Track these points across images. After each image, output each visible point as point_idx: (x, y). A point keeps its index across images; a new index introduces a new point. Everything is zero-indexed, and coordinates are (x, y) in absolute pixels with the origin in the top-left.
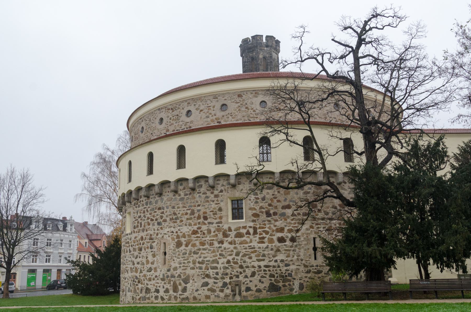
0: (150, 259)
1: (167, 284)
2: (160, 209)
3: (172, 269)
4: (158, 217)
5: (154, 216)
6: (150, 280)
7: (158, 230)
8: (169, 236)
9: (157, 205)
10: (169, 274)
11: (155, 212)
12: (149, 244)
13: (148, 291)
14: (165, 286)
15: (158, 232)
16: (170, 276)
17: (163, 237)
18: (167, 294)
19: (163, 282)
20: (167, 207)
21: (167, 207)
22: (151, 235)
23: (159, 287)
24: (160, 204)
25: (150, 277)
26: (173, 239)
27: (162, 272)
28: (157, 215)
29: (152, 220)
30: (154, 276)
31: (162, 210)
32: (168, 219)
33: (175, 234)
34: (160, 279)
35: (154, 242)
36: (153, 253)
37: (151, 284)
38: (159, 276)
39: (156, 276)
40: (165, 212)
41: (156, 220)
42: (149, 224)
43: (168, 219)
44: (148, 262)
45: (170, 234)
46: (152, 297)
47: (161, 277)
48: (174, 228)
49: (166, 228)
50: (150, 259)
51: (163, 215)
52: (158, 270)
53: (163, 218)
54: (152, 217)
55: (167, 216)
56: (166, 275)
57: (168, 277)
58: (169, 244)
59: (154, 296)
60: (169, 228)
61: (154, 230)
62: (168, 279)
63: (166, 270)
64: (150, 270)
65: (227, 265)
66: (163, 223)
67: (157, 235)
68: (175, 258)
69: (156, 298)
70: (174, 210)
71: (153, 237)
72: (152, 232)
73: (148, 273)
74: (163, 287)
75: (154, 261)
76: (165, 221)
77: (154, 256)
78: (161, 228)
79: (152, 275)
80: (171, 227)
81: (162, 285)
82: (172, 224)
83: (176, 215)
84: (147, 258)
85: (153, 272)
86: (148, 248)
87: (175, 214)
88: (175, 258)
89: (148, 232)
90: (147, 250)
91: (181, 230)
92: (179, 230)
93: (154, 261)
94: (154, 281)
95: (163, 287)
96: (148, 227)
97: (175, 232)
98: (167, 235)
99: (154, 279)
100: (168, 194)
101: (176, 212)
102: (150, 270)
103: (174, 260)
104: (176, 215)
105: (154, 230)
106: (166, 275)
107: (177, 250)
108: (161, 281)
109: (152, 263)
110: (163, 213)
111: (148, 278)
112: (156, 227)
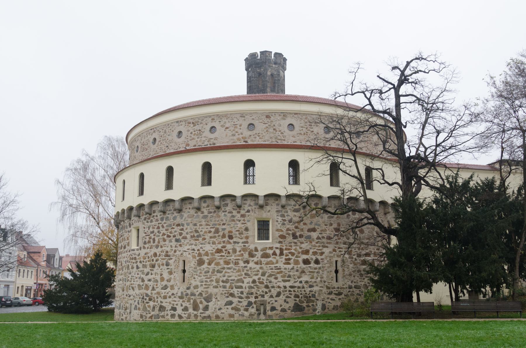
0: (166, 276)
1: (186, 302)
2: (178, 225)
3: (192, 287)
4: (176, 233)
5: (171, 233)
6: (165, 297)
7: (176, 247)
8: (189, 254)
9: (175, 221)
10: (189, 292)
11: (173, 228)
12: (164, 262)
13: (162, 308)
14: (183, 304)
15: (176, 249)
16: (189, 294)
17: (182, 254)
18: (186, 312)
19: (181, 300)
20: (188, 224)
21: (188, 224)
22: (167, 252)
23: (177, 305)
24: (178, 220)
25: (166, 294)
26: (194, 257)
27: (181, 290)
28: (176, 232)
29: (169, 236)
30: (170, 294)
31: (182, 227)
32: (188, 236)
33: (196, 251)
34: (177, 297)
35: (171, 259)
36: (169, 270)
37: (166, 302)
38: (177, 293)
39: (173, 294)
40: (185, 229)
41: (174, 236)
42: (164, 240)
43: (188, 236)
44: (162, 279)
45: (191, 252)
46: (167, 315)
47: (179, 294)
48: (196, 245)
49: (186, 245)
50: (166, 276)
51: (182, 232)
52: (176, 288)
53: (183, 235)
54: (169, 233)
55: (187, 233)
56: (184, 293)
57: (187, 295)
58: (189, 262)
59: (170, 315)
60: (189, 245)
61: (171, 246)
62: (188, 297)
63: (185, 288)
64: (165, 287)
65: (252, 285)
66: (182, 240)
67: (175, 251)
68: (196, 277)
69: (173, 316)
70: (196, 227)
71: (169, 253)
72: (168, 249)
73: (163, 291)
74: (182, 305)
75: (171, 278)
76: (185, 238)
77: (170, 273)
78: (180, 245)
79: (168, 293)
80: (192, 244)
81: (179, 303)
82: (193, 242)
83: (198, 232)
84: (161, 275)
85: (169, 289)
86: (163, 265)
87: (196, 231)
88: (196, 277)
89: (164, 248)
90: (161, 268)
91: (204, 249)
92: (201, 248)
93: (171, 278)
94: (171, 299)
95: (182, 305)
96: (164, 243)
97: (196, 249)
98: (187, 253)
99: (170, 297)
100: (190, 210)
101: (197, 229)
102: (165, 287)
103: (194, 278)
104: (198, 232)
105: (171, 246)
106: (184, 293)
107: (198, 268)
108: (179, 300)
109: (169, 281)
110: (182, 230)
111: (162, 295)
112: (174, 243)
